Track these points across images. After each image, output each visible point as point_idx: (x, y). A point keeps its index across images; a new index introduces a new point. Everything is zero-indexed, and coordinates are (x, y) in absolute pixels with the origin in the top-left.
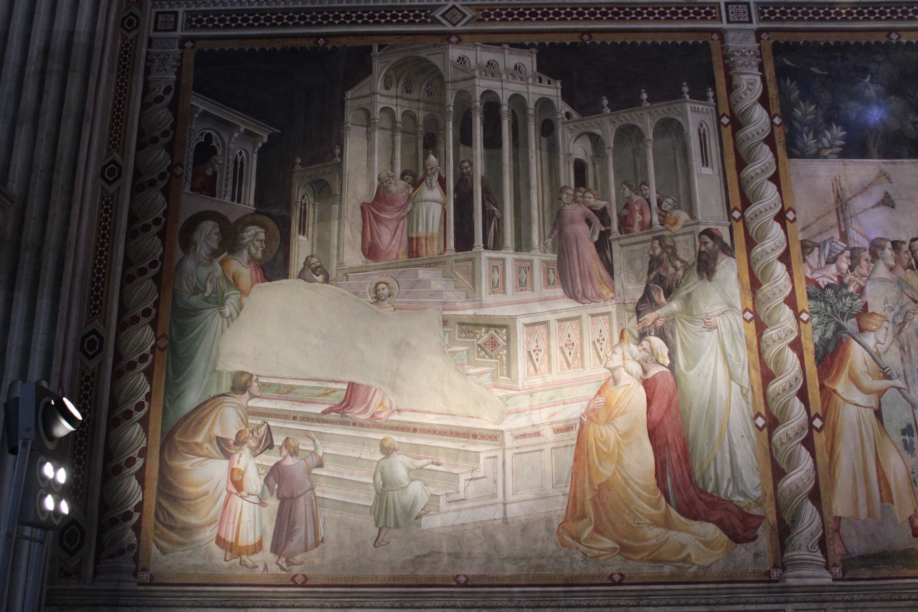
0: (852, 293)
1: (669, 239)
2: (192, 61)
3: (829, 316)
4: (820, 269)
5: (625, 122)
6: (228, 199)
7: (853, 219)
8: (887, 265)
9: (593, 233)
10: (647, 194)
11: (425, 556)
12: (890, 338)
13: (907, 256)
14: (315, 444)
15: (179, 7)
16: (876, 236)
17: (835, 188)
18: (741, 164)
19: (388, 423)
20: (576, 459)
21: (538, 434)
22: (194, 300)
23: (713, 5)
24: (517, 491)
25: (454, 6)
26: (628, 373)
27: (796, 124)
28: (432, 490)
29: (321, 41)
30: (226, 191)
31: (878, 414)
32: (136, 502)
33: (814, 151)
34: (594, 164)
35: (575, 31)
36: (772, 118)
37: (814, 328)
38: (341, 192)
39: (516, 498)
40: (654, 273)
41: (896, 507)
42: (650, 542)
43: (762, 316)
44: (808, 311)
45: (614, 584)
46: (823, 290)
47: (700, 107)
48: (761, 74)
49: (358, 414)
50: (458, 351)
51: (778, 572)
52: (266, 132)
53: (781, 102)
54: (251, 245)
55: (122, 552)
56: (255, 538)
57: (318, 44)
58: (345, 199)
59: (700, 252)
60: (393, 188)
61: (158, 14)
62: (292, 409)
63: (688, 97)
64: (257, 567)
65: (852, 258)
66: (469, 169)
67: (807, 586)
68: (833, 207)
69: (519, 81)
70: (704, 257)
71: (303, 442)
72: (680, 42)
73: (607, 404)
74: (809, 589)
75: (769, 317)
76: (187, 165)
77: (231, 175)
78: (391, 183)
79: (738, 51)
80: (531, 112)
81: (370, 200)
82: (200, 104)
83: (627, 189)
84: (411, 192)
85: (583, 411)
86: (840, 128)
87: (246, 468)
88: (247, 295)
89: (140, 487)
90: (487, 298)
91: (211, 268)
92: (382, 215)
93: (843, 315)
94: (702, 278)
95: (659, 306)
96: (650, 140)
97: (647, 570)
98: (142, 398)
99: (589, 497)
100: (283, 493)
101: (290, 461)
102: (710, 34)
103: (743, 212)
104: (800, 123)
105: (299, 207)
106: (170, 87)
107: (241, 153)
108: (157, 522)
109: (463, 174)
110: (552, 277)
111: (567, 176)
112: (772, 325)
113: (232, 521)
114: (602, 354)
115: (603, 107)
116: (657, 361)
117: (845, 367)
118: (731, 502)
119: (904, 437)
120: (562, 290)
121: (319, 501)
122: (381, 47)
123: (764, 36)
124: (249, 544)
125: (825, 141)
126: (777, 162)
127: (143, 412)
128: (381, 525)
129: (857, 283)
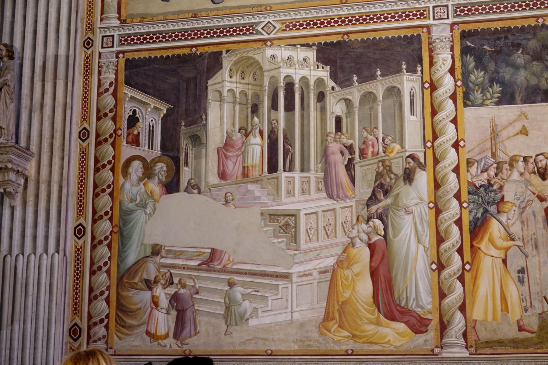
0: (495, 190)
1: (388, 161)
2: (123, 66)
4: (477, 176)
5: (366, 90)
6: (146, 148)
8: (518, 171)
9: (345, 160)
10: (376, 134)
11: (250, 340)
12: (516, 217)
13: (532, 166)
14: (194, 282)
15: (114, 32)
17: (491, 124)
18: (434, 113)
20: (330, 288)
21: (310, 275)
22: (131, 206)
23: (425, 9)
24: (298, 305)
25: (269, 22)
26: (360, 240)
27: (471, 85)
28: (254, 305)
29: (194, 50)
30: (145, 143)
31: (504, 261)
32: (106, 314)
33: (480, 101)
34: (347, 118)
35: (339, 33)
36: (456, 82)
37: (470, 212)
38: (206, 141)
39: (298, 309)
40: (378, 182)
42: (367, 334)
43: (439, 206)
44: (468, 201)
45: (348, 355)
46: (478, 189)
47: (412, 77)
48: (451, 53)
50: (269, 230)
51: (438, 350)
52: (165, 107)
53: (462, 71)
55: (100, 339)
57: (192, 51)
58: (209, 146)
59: (406, 168)
60: (234, 138)
61: (103, 37)
63: (405, 71)
64: (166, 346)
65: (497, 168)
66: (276, 125)
67: (454, 358)
68: (489, 137)
69: (306, 68)
70: (408, 171)
71: (189, 281)
72: (402, 36)
73: (348, 257)
75: (444, 205)
76: (124, 129)
77: (147, 134)
78: (233, 135)
79: (438, 39)
80: (312, 87)
81: (222, 146)
82: (128, 92)
83: (365, 132)
84: (244, 140)
85: (335, 261)
86: (498, 85)
87: (160, 295)
88: (158, 202)
90: (284, 199)
93: (488, 203)
94: (405, 184)
95: (380, 201)
96: (380, 101)
97: (367, 348)
98: (107, 259)
99: (337, 307)
101: (182, 291)
102: (422, 28)
103: (433, 143)
104: (473, 84)
106: (112, 82)
107: (152, 121)
108: (116, 324)
109: (273, 128)
110: (321, 186)
111: (331, 126)
112: (446, 210)
113: (153, 323)
114: (346, 230)
115: (354, 82)
116: (377, 233)
118: (414, 311)
119: (519, 275)
120: (325, 194)
122: (227, 51)
123: (456, 27)
125: (488, 95)
126: (456, 110)
128: (228, 324)
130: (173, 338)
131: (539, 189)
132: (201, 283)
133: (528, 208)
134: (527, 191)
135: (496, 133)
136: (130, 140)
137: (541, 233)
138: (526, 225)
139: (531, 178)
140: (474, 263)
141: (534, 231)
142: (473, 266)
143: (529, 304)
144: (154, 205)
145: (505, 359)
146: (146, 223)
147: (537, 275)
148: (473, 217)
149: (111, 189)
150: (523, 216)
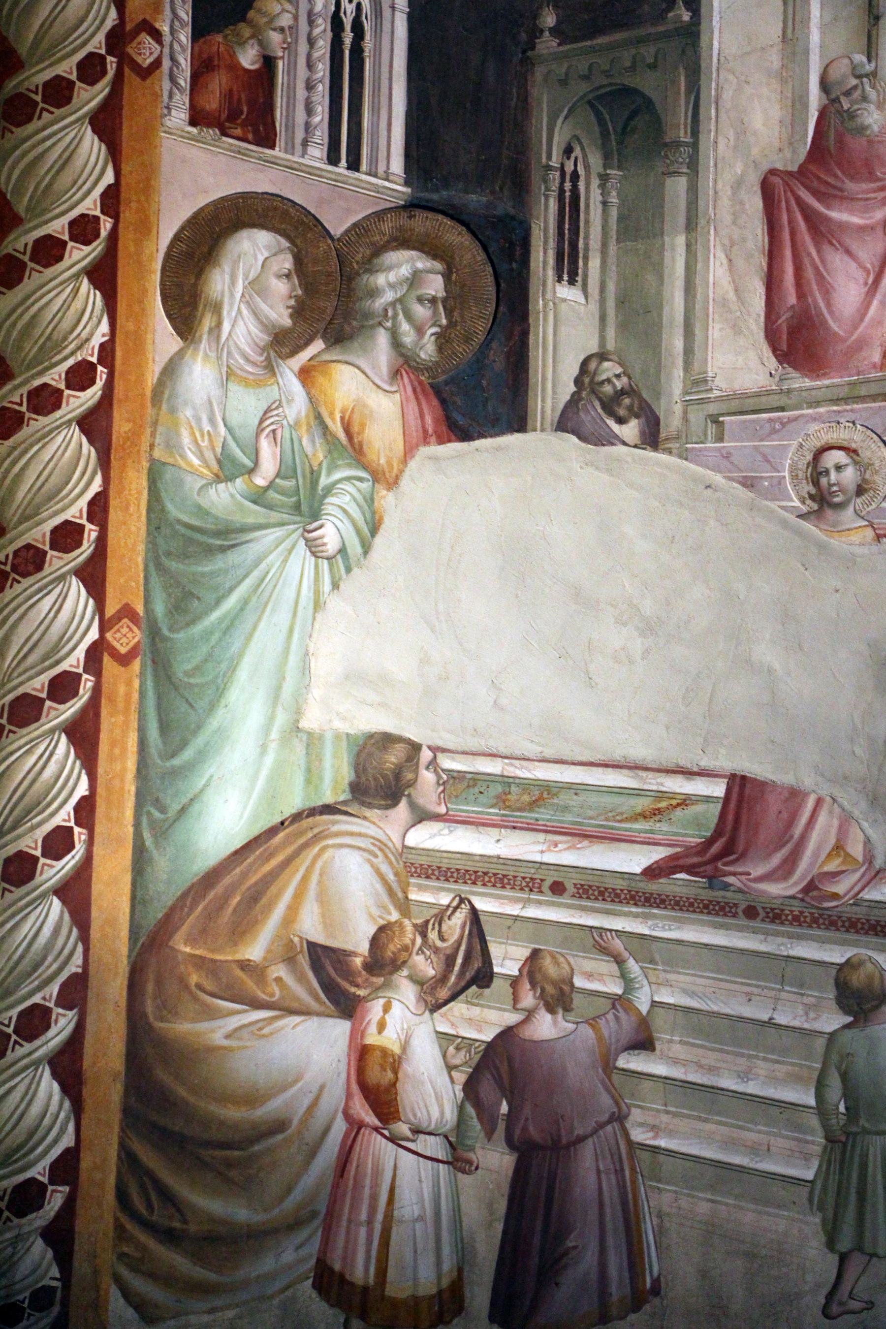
6: (317, 153)
14: (624, 976)
19: (860, 912)
30: (307, 125)
38: (695, 133)
49: (760, 879)
54: (401, 316)
56: (439, 1277)
62: (549, 858)
71: (589, 965)
77: (323, 69)
78: (865, 98)
87: (405, 1046)
88: (393, 484)
89: (67, 1104)
91: (273, 392)
92: (834, 215)
98: (64, 816)
100: (525, 1129)
105: (555, 186)
113: (364, 1216)
121: (645, 1156)
124: (421, 1292)
127: (70, 862)
128: (845, 1243)
130: (492, 1318)
132: (668, 984)
136: (212, 102)
144: (370, 500)
146: (318, 605)
149: (93, 394)
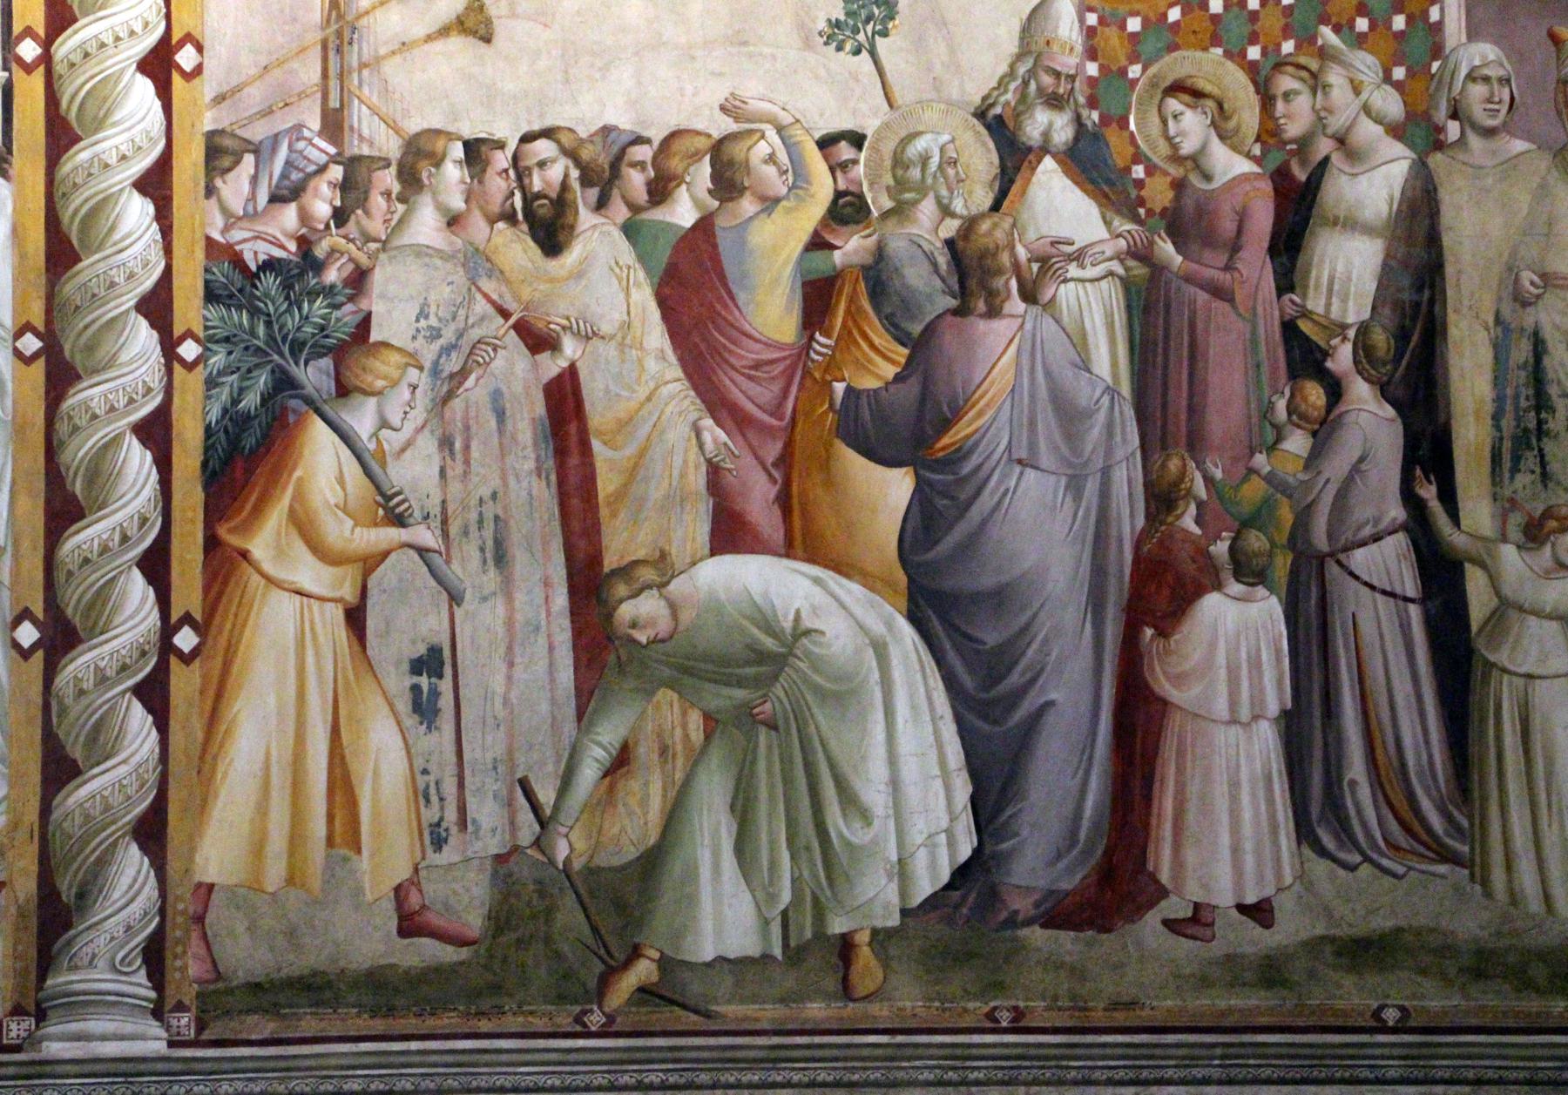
0: (332, 287)
3: (258, 349)
4: (251, 216)
7: (365, 72)
8: (441, 208)
12: (418, 415)
16: (426, 126)
31: (355, 618)
37: (211, 383)
41: (364, 863)
43: (67, 348)
44: (201, 335)
51: (25, 1025)
65: (345, 186)
74: (98, 1068)
75: (90, 348)
93: (297, 347)
103: (47, 43)
112: (96, 371)
117: (284, 488)
119: (416, 679)
129: (351, 260)
131: (526, 293)
133: (472, 378)
134: (471, 299)
135: (349, 18)
137: (524, 493)
138: (459, 456)
139: (497, 240)
140: (217, 620)
141: (496, 482)
142: (213, 630)
143: (451, 815)
145: (333, 1062)
147: (498, 683)
148: (225, 411)
150: (448, 414)
